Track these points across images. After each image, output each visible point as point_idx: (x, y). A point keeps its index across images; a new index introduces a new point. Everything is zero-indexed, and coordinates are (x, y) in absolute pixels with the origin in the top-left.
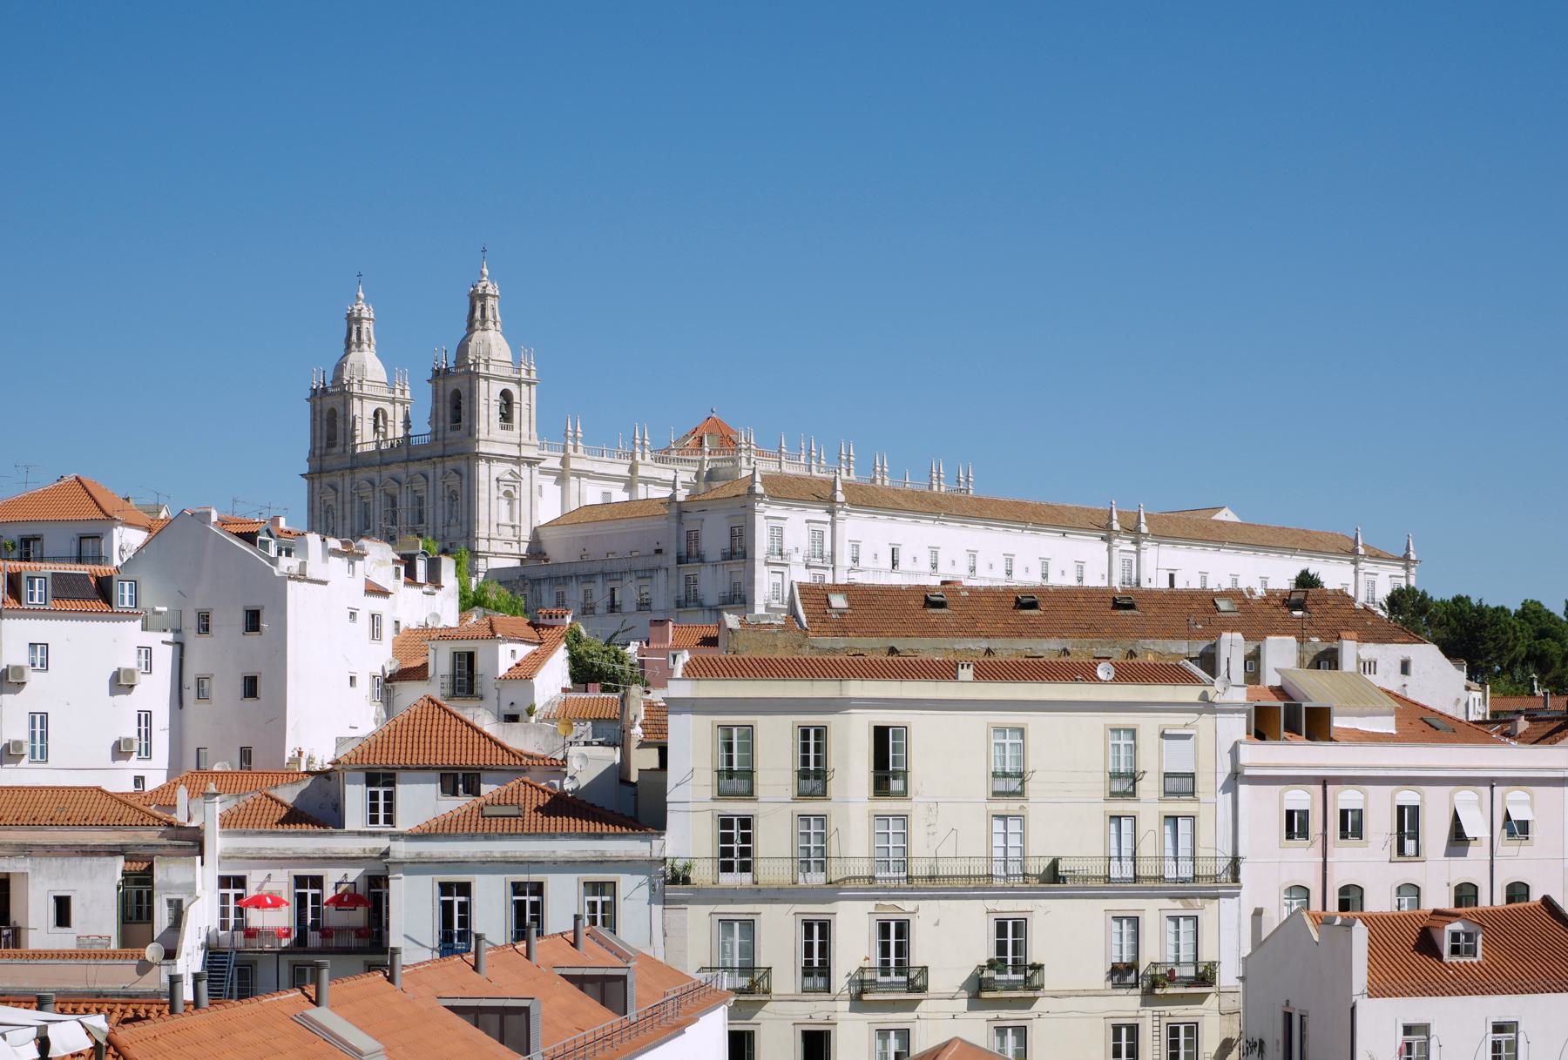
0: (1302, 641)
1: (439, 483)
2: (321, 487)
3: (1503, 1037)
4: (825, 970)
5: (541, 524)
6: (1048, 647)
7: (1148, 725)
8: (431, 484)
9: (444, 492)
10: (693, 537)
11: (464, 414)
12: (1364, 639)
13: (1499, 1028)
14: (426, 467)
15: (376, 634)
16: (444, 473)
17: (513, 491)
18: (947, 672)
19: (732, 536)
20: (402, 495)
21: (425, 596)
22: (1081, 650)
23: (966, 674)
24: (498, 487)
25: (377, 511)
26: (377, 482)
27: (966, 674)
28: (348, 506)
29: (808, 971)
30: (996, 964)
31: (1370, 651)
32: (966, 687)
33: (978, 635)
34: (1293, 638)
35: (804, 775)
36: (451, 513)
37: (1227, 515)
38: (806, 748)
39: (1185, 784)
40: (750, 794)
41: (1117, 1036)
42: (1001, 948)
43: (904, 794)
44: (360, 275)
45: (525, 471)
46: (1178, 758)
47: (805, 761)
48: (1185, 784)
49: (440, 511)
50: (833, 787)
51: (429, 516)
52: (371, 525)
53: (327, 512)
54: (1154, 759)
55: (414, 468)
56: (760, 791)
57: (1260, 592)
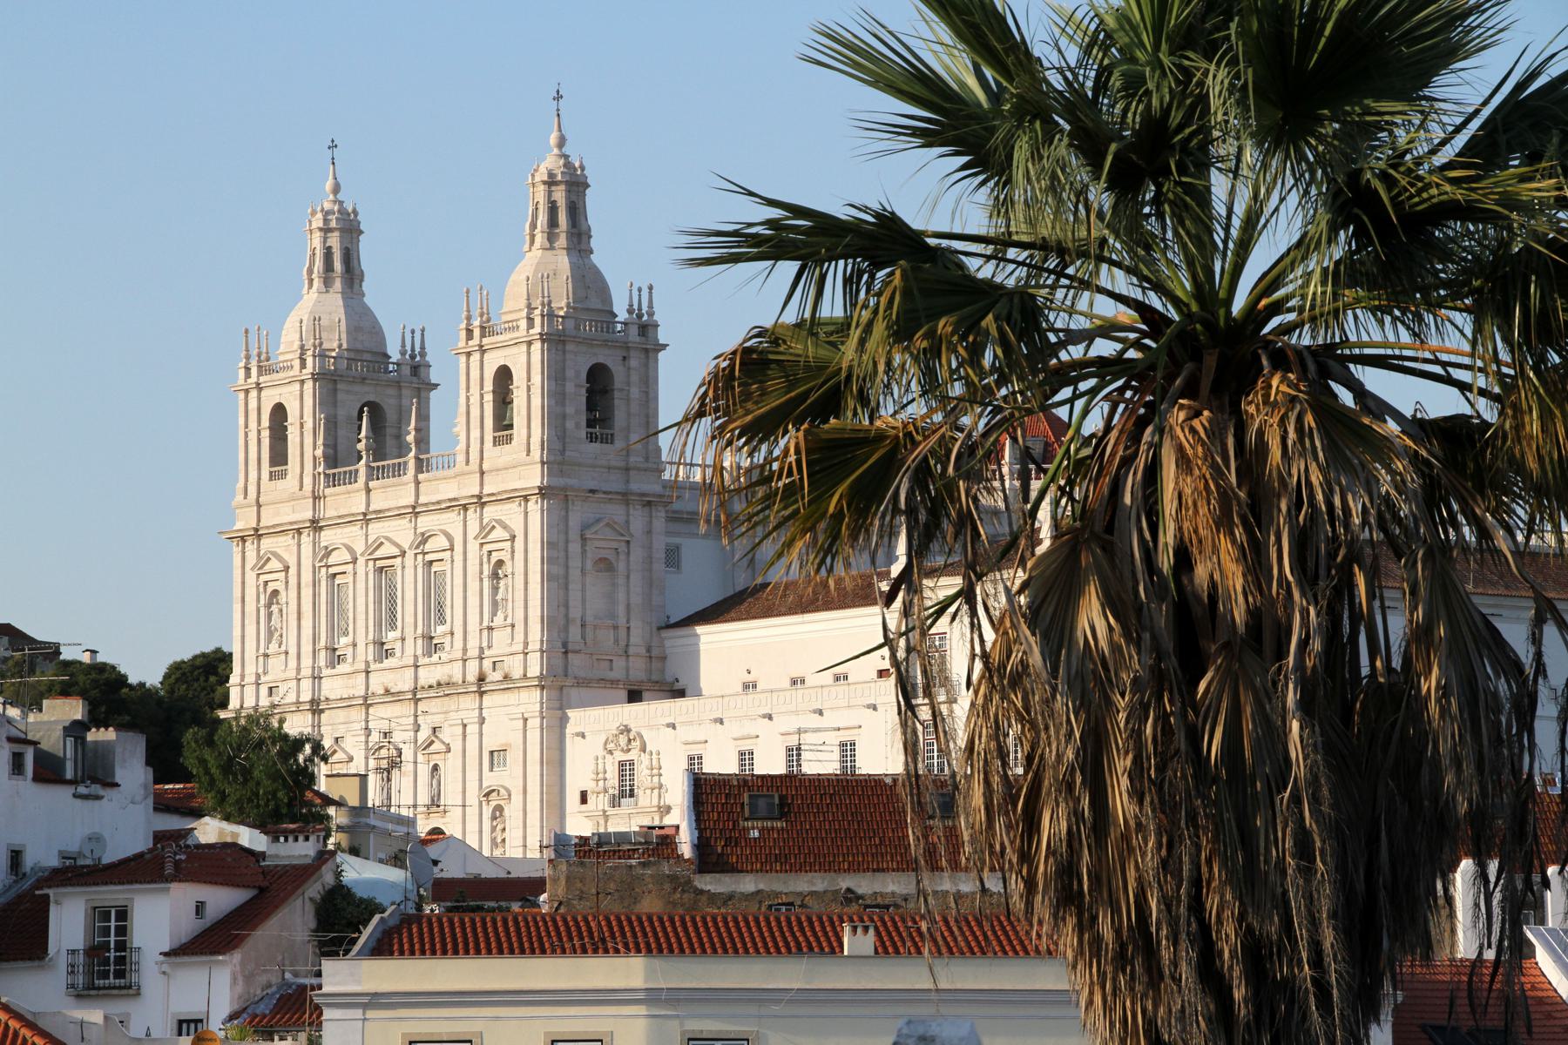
1: (473, 546)
2: (259, 557)
5: (672, 621)
8: (458, 548)
9: (481, 564)
11: (519, 414)
14: (452, 521)
16: (482, 528)
17: (610, 556)
20: (407, 570)
21: (78, 802)
24: (584, 552)
25: (361, 601)
26: (359, 547)
44: (333, 146)
51: (454, 613)
52: (351, 629)
53: (269, 605)
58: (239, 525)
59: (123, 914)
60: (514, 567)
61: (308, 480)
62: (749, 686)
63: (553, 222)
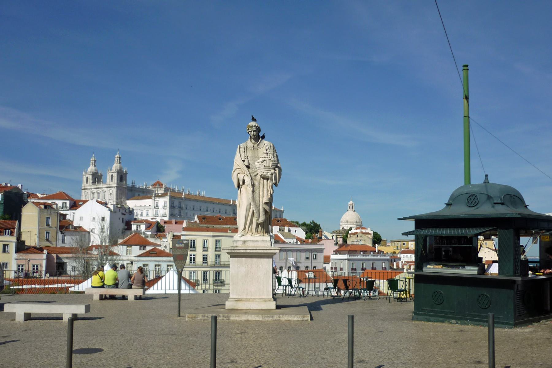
4: (206, 280)
10: (157, 203)
15: (123, 222)
19: (165, 204)
28: (90, 195)
29: (204, 280)
31: (291, 228)
33: (227, 225)
35: (204, 247)
36: (110, 197)
38: (204, 243)
40: (195, 251)
47: (204, 245)
49: (108, 197)
50: (209, 250)
55: (103, 189)
58: (82, 188)
59: (140, 226)
60: (113, 193)
61: (90, 184)
63: (117, 161)
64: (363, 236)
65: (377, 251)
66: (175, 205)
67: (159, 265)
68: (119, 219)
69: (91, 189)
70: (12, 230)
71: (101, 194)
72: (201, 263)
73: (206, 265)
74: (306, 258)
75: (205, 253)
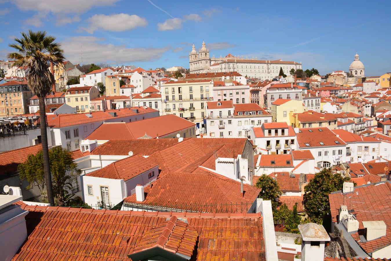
0: (230, 76)
3: (220, 113)
4: (175, 108)
6: (207, 78)
7: (204, 86)
10: (222, 66)
12: (236, 76)
13: (220, 112)
18: (185, 82)
22: (209, 79)
23: (187, 82)
27: (187, 82)
30: (191, 107)
31: (237, 77)
32: (187, 83)
34: (229, 77)
37: (281, 60)
39: (208, 91)
40: (168, 94)
41: (202, 113)
42: (191, 106)
43: (181, 93)
45: (208, 61)
46: (207, 88)
48: (208, 91)
54: (204, 88)
56: (169, 93)
57: (229, 72)
62: (214, 69)
64: (337, 76)
65: (292, 87)
66: (230, 66)
67: (151, 103)
68: (150, 79)
69: (193, 62)
70: (89, 90)
71: (198, 64)
72: (172, 100)
73: (174, 101)
74: (230, 94)
75: (173, 95)
